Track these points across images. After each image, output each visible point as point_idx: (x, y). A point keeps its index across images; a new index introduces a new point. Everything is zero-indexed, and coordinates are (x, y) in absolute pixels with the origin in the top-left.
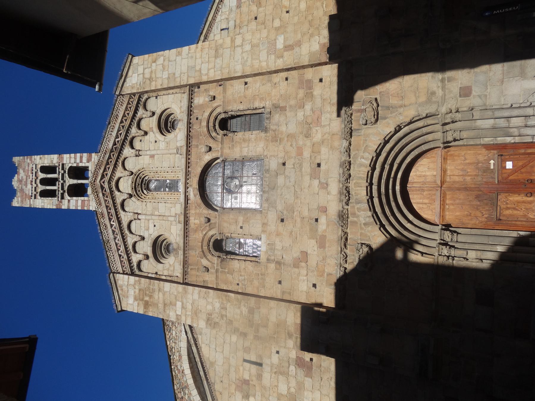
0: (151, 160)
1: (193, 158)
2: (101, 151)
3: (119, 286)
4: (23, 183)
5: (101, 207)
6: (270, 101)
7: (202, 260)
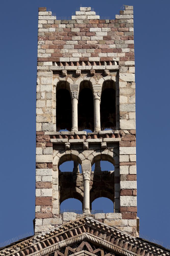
4: (85, 38)
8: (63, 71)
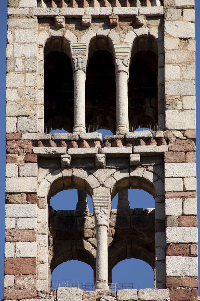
8: (57, 17)
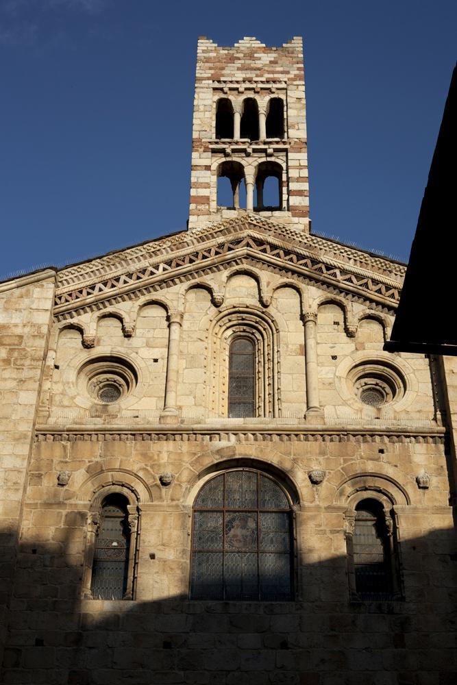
0: (294, 348)
1: (297, 446)
2: (313, 238)
3: (28, 291)
4: (248, 62)
5: (195, 241)
6: (414, 613)
7: (83, 471)
